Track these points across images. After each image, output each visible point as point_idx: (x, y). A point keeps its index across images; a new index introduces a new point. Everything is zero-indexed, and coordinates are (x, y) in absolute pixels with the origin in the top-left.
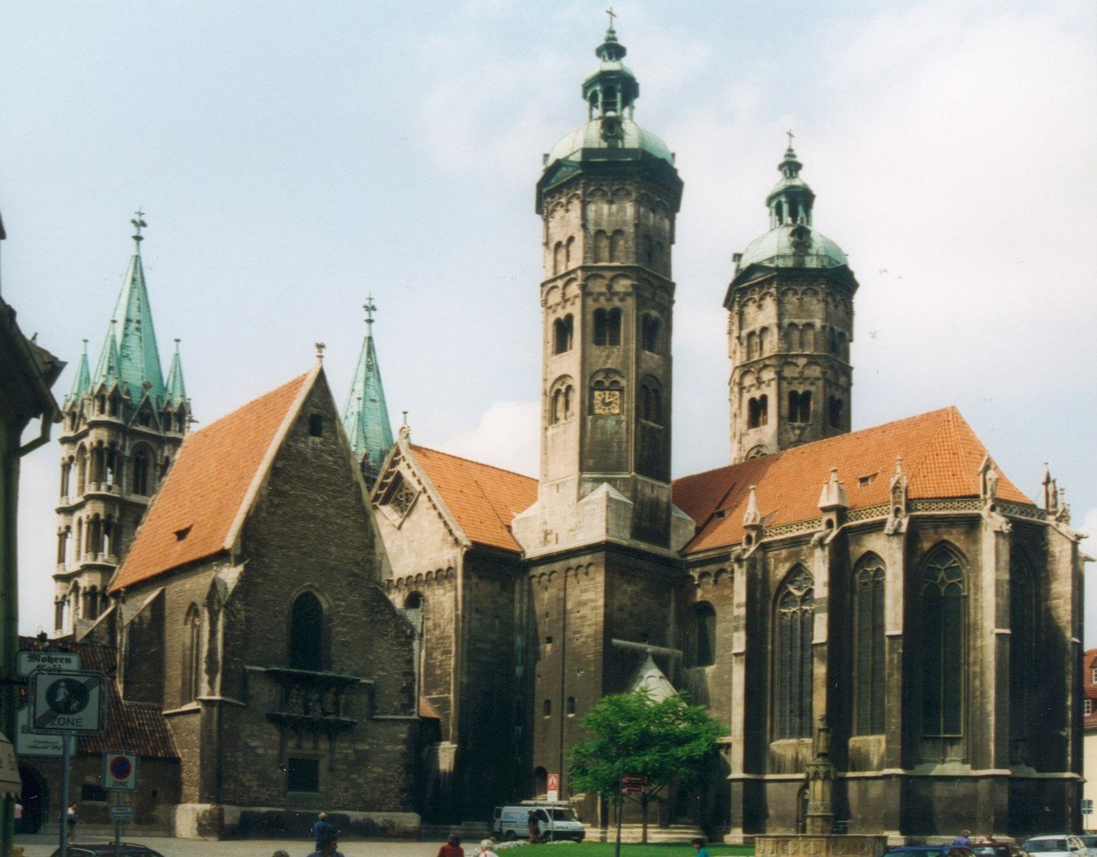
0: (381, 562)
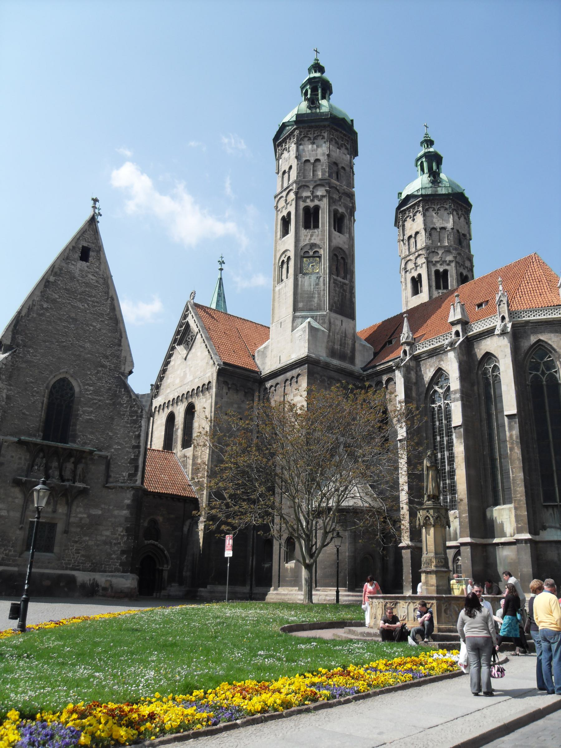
0: (126, 357)
